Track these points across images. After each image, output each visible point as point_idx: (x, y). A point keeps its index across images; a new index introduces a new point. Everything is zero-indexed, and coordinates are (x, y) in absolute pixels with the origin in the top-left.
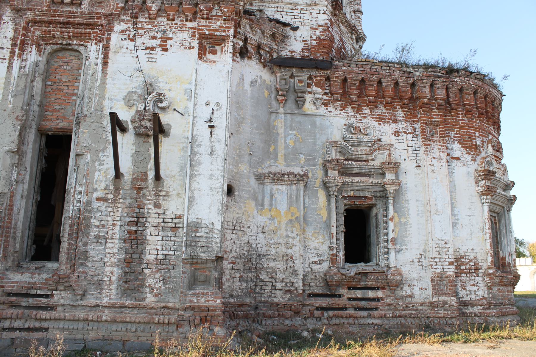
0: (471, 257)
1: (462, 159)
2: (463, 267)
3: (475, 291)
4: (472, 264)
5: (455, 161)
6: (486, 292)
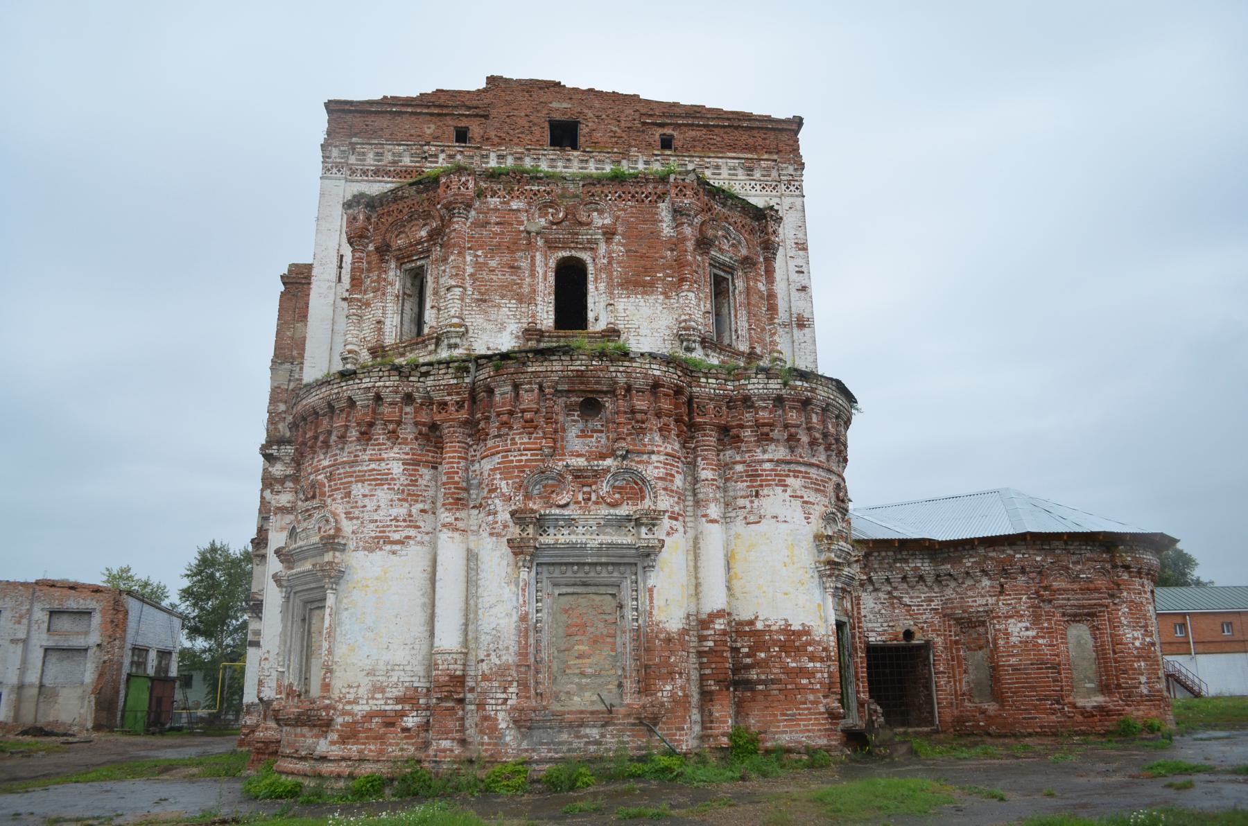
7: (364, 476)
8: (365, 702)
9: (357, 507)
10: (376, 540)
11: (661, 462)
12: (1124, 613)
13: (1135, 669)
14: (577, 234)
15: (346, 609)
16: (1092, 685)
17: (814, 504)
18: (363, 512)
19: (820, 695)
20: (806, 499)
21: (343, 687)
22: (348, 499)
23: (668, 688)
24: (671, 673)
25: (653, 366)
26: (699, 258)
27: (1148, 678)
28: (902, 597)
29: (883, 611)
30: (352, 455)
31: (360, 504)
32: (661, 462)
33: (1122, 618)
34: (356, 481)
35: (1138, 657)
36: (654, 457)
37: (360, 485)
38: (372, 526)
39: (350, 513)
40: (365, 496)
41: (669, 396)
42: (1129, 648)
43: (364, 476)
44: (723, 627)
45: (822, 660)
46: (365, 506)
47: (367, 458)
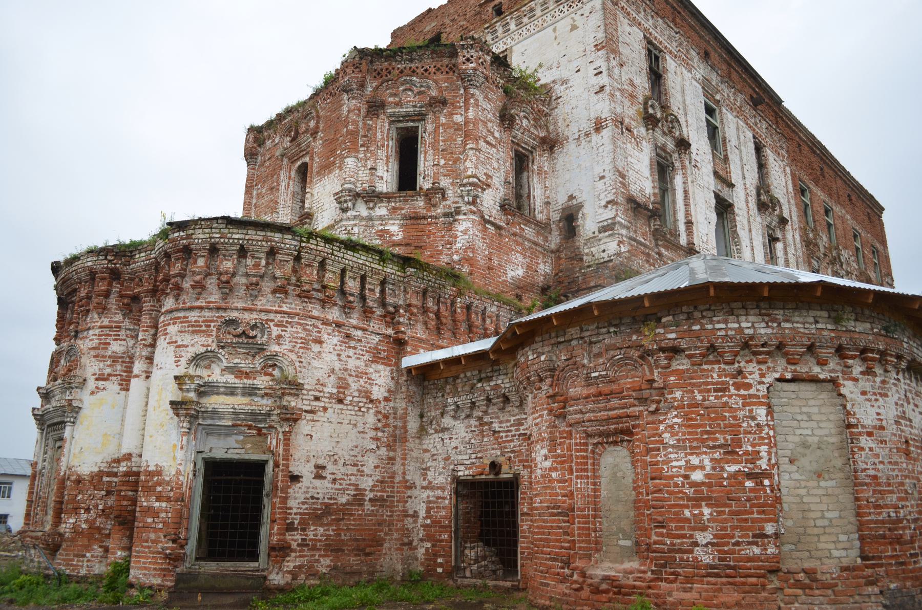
11: (95, 335)
12: (672, 427)
13: (687, 520)
14: (300, 144)
16: (628, 543)
17: (187, 346)
19: (161, 535)
20: (179, 343)
23: (71, 521)
24: (76, 509)
25: (88, 260)
26: (371, 122)
27: (715, 536)
28: (492, 423)
29: (473, 441)
32: (95, 335)
33: (666, 435)
35: (697, 501)
36: (91, 332)
41: (105, 279)
42: (676, 485)
44: (125, 469)
45: (168, 500)
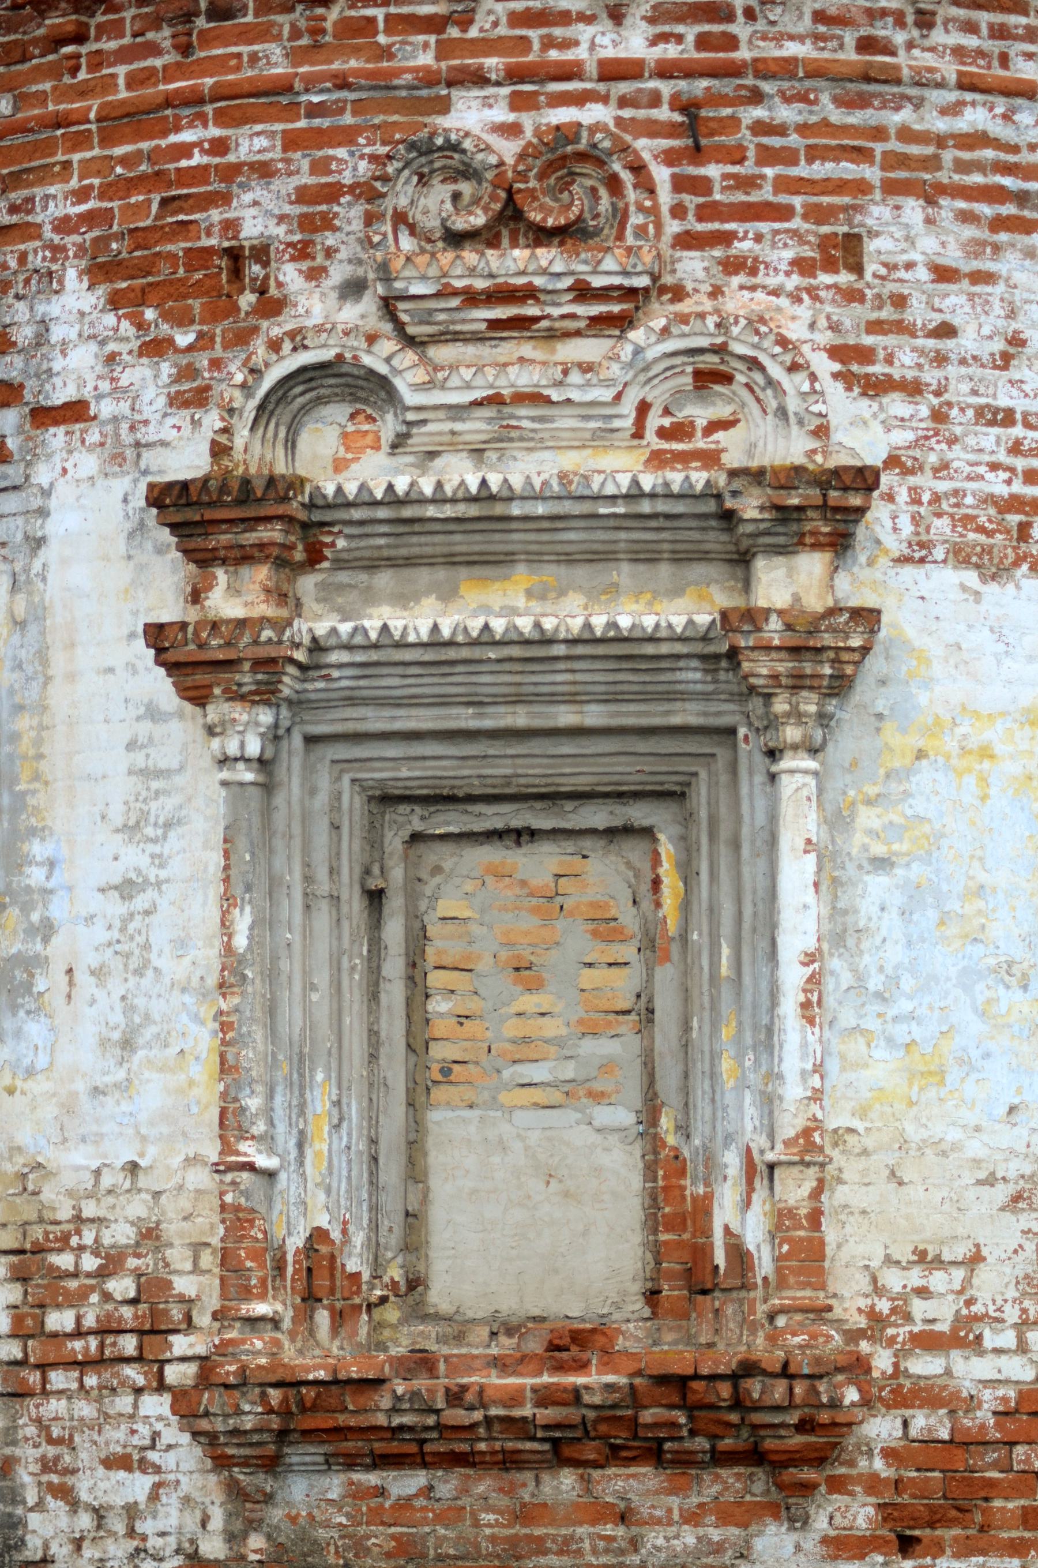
0: (122, 1234)
1: (106, 409)
2: (60, 1320)
3: (131, 1511)
4: (122, 1286)
5: (56, 436)
6: (217, 1522)
7: (932, 163)
8: (1008, 1339)
9: (900, 328)
10: (1014, 519)
15: (882, 864)
18: (940, 359)
21: (889, 1261)
22: (844, 278)
30: (850, 38)
31: (917, 313)
34: (891, 188)
37: (913, 209)
38: (990, 438)
39: (866, 355)
40: (944, 274)
43: (932, 163)
46: (946, 331)
47: (949, 69)
